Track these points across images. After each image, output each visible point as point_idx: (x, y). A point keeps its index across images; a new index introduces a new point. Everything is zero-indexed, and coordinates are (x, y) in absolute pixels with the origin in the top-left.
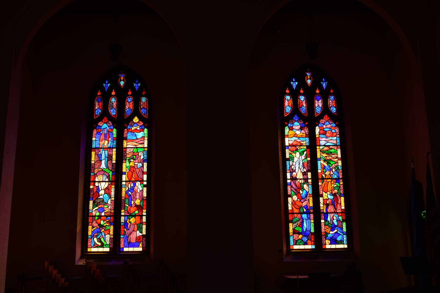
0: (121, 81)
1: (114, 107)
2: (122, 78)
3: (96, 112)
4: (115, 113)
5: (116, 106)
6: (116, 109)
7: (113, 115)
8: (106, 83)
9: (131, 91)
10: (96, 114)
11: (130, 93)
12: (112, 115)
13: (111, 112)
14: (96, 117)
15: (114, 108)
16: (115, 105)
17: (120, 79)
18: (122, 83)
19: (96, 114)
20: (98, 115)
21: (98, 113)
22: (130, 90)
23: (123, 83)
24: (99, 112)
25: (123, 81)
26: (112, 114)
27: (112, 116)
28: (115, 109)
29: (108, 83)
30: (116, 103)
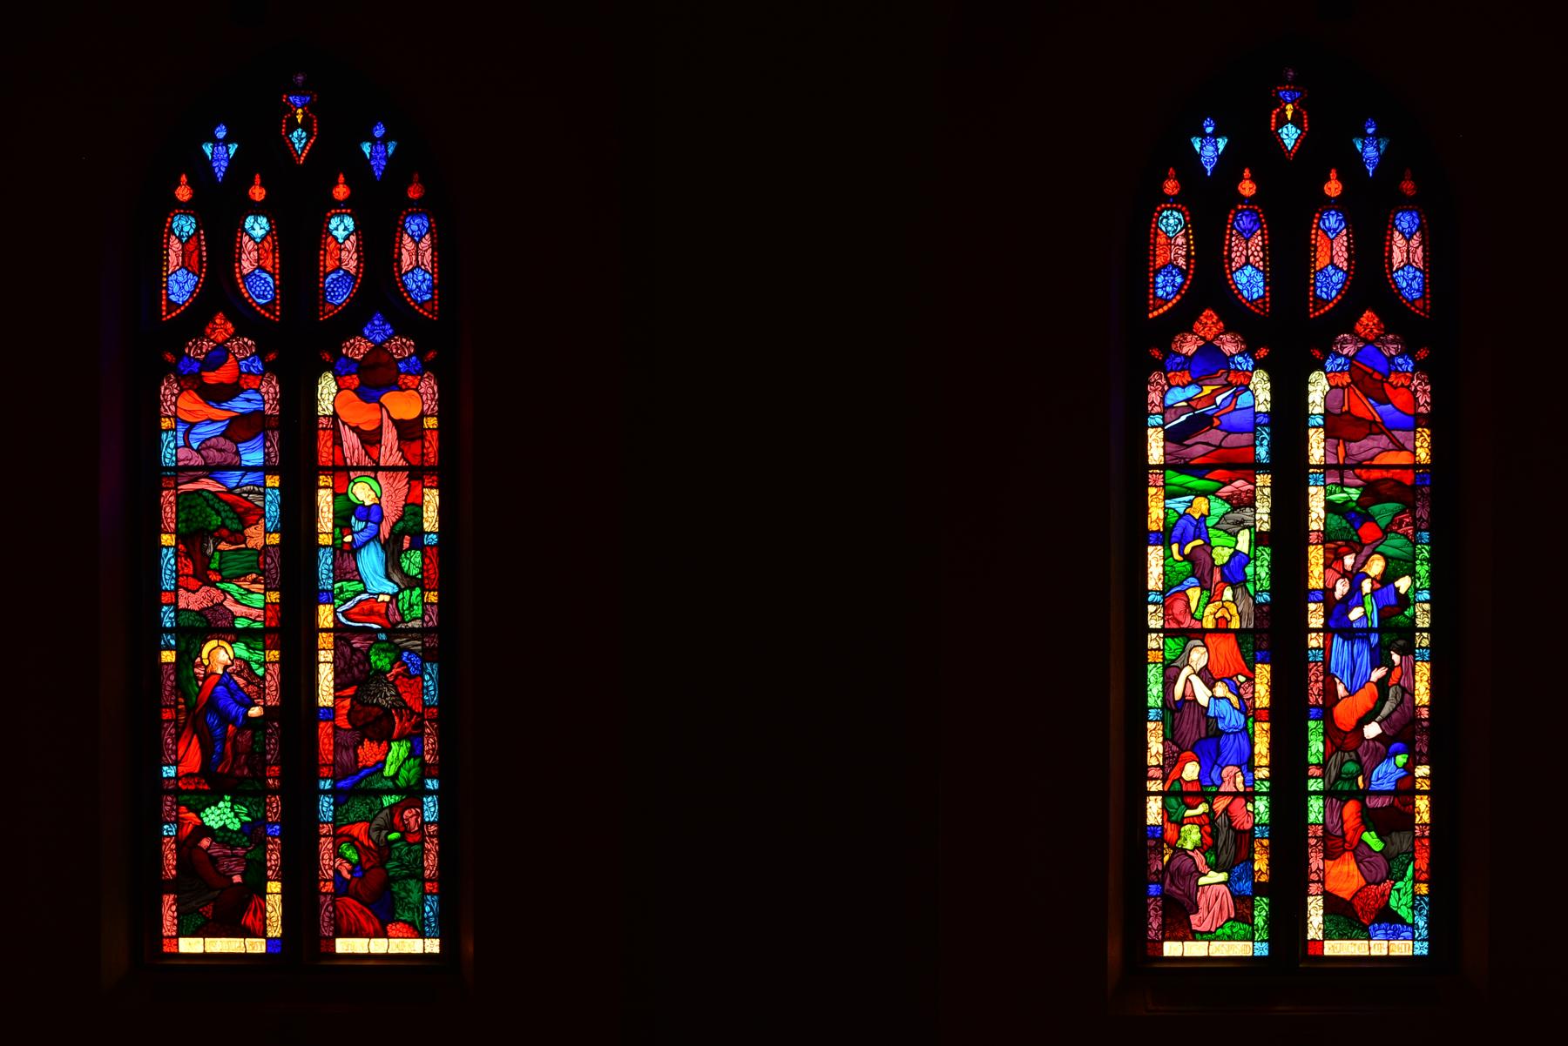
0: (1282, 122)
1: (1251, 258)
2: (1289, 107)
3: (1155, 283)
4: (1261, 292)
5: (1261, 254)
6: (1264, 272)
7: (1247, 299)
8: (1203, 135)
9: (1339, 178)
10: (1160, 293)
11: (1333, 188)
12: (1244, 301)
13: (1240, 287)
14: (1161, 307)
15: (1253, 266)
16: (1259, 248)
17: (1278, 115)
18: (1290, 135)
19: (1160, 293)
20: (1170, 300)
21: (1169, 289)
22: (1333, 174)
23: (1296, 136)
24: (1173, 286)
25: (1296, 121)
26: (1245, 293)
27: (1248, 305)
28: (1257, 269)
29: (1215, 135)
30: (1263, 241)
